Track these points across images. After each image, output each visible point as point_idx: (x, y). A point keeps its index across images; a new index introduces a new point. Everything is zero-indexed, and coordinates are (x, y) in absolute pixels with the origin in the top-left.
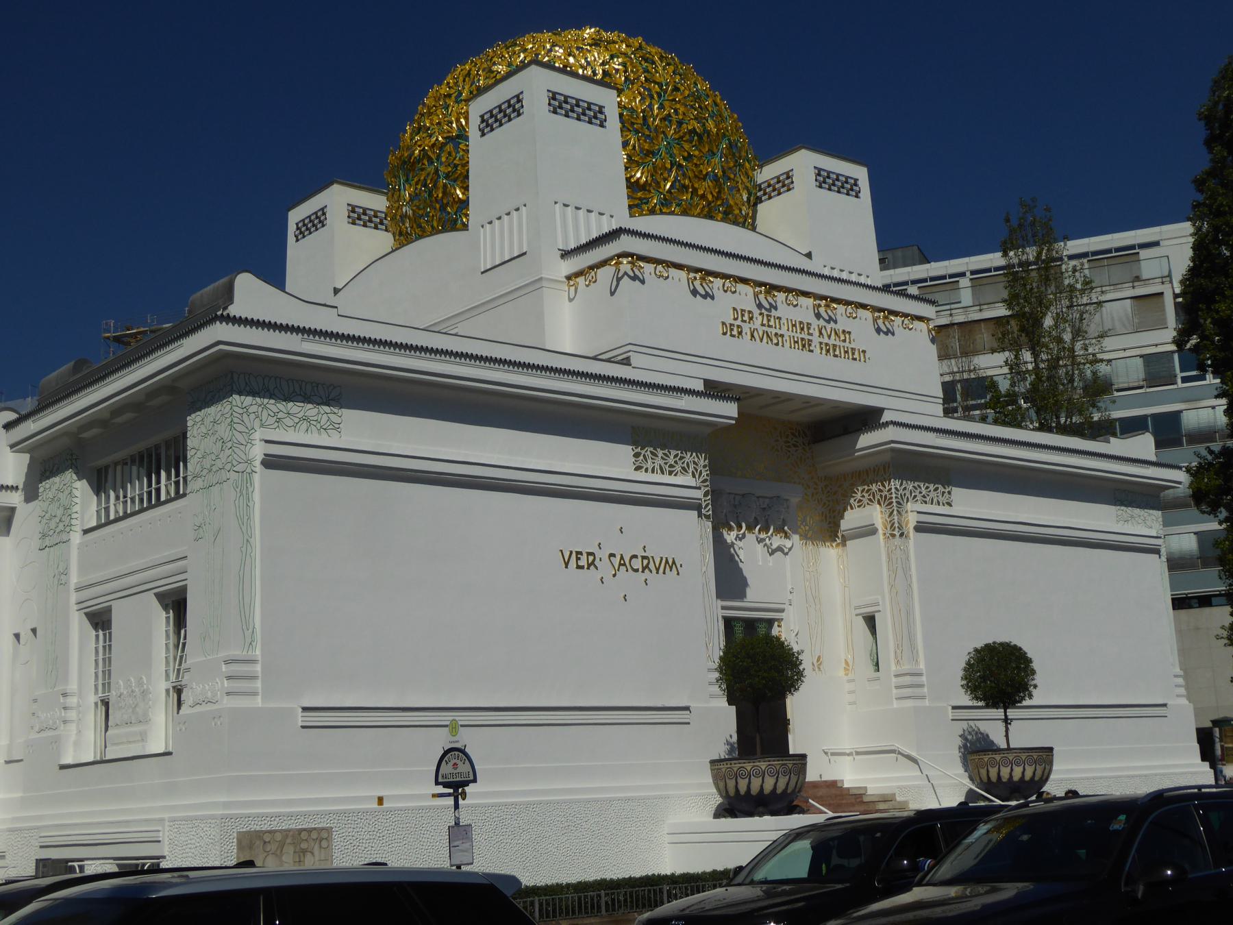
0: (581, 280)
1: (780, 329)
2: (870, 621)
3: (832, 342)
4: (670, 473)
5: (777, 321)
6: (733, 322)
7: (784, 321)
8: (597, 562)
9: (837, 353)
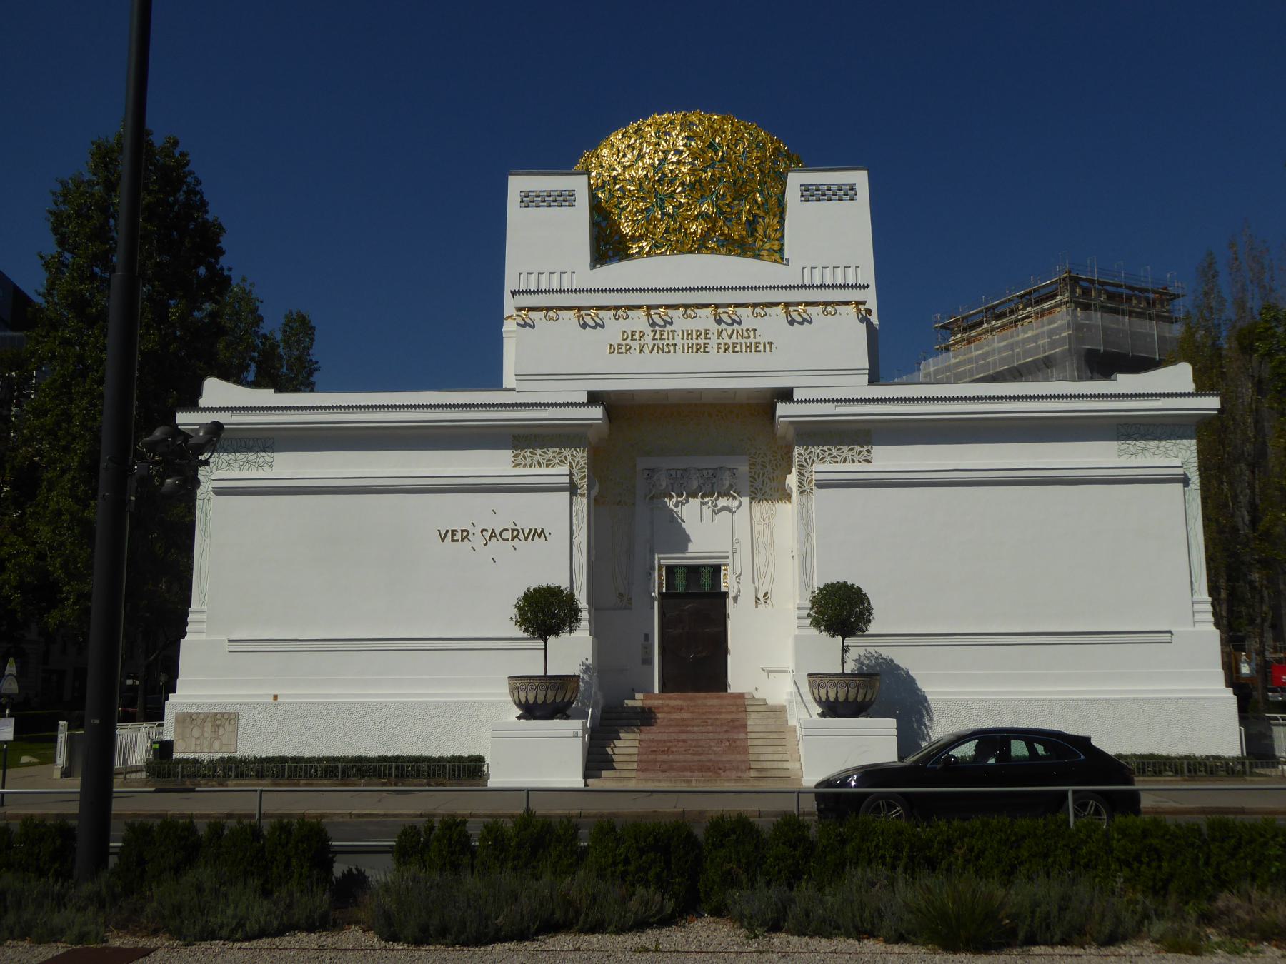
1: (673, 339)
4: (548, 466)
5: (671, 334)
9: (738, 349)
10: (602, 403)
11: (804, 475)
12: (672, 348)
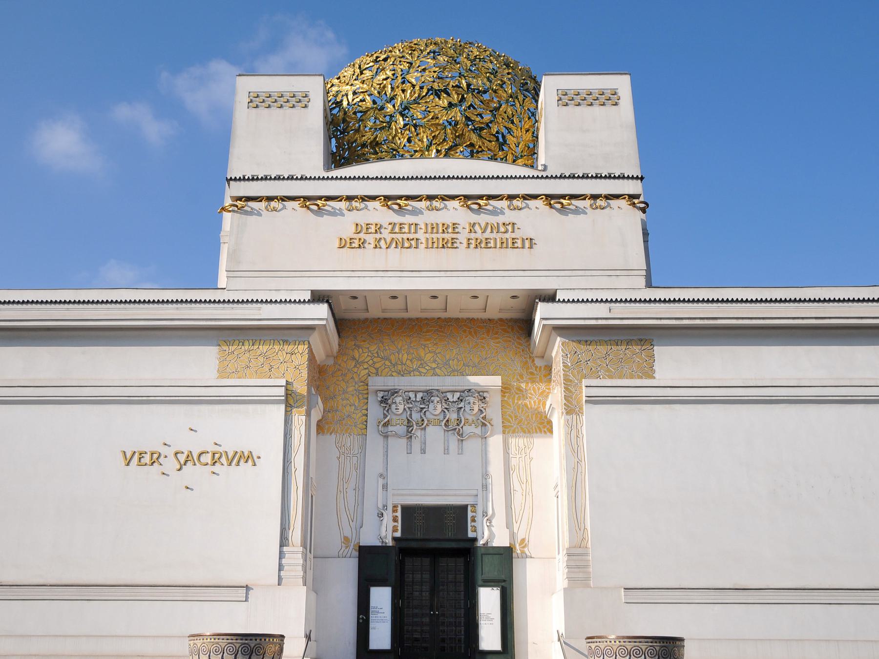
3: (488, 234)
5: (413, 227)
6: (356, 236)
8: (161, 460)
9: (492, 245)
10: (327, 302)
11: (571, 392)
12: (413, 243)
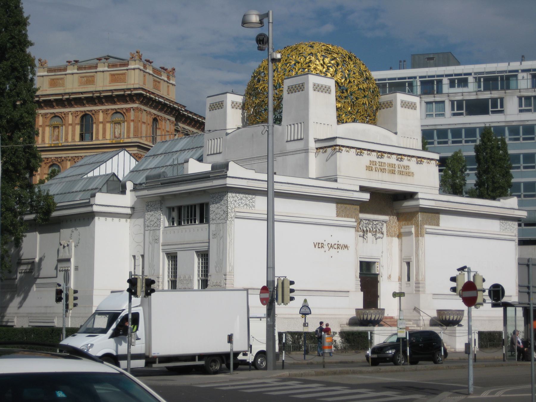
0: (321, 150)
2: (408, 264)
3: (403, 170)
7: (386, 164)
8: (324, 246)
9: (403, 174)
